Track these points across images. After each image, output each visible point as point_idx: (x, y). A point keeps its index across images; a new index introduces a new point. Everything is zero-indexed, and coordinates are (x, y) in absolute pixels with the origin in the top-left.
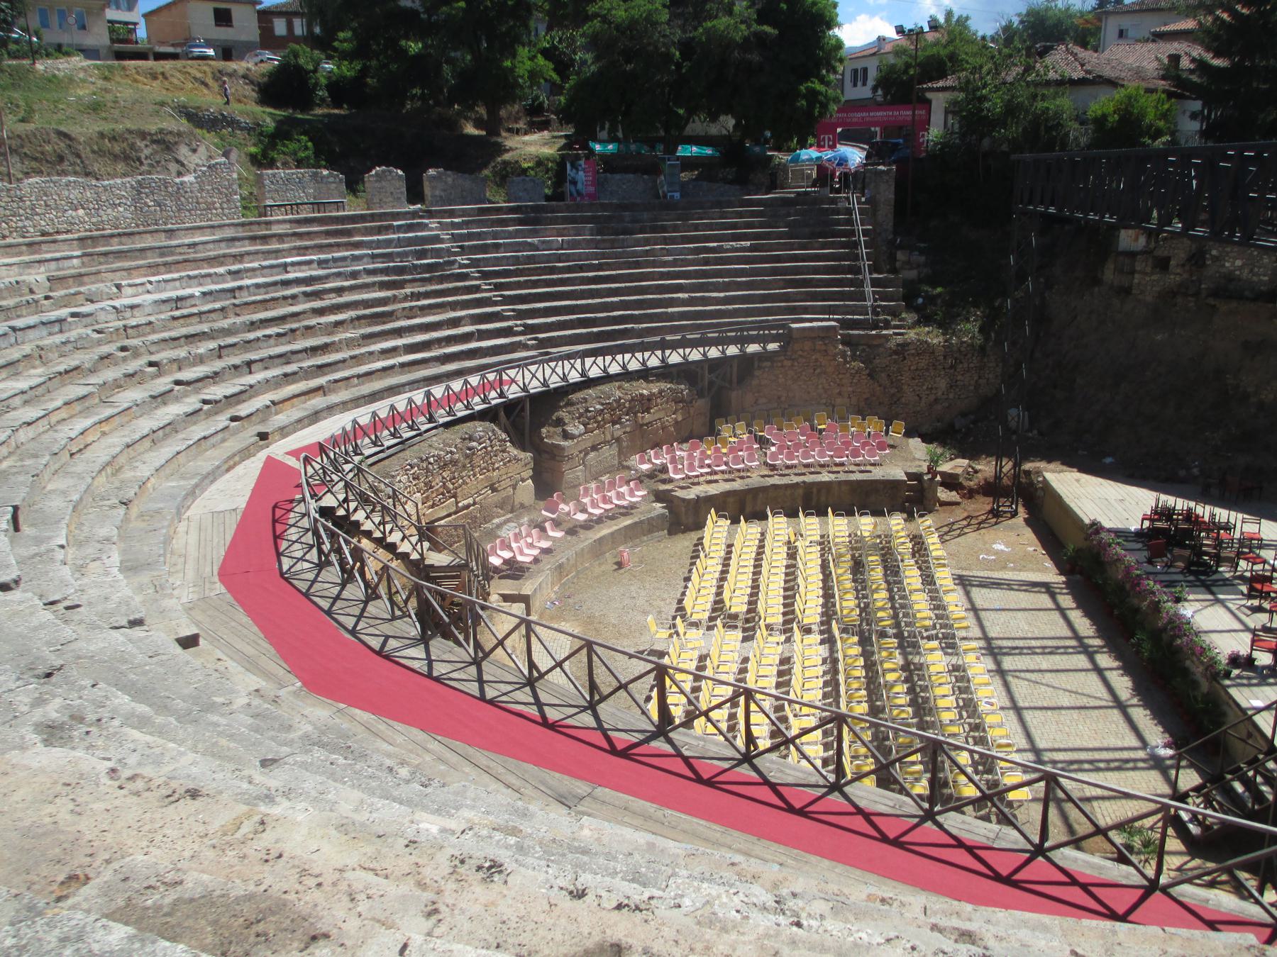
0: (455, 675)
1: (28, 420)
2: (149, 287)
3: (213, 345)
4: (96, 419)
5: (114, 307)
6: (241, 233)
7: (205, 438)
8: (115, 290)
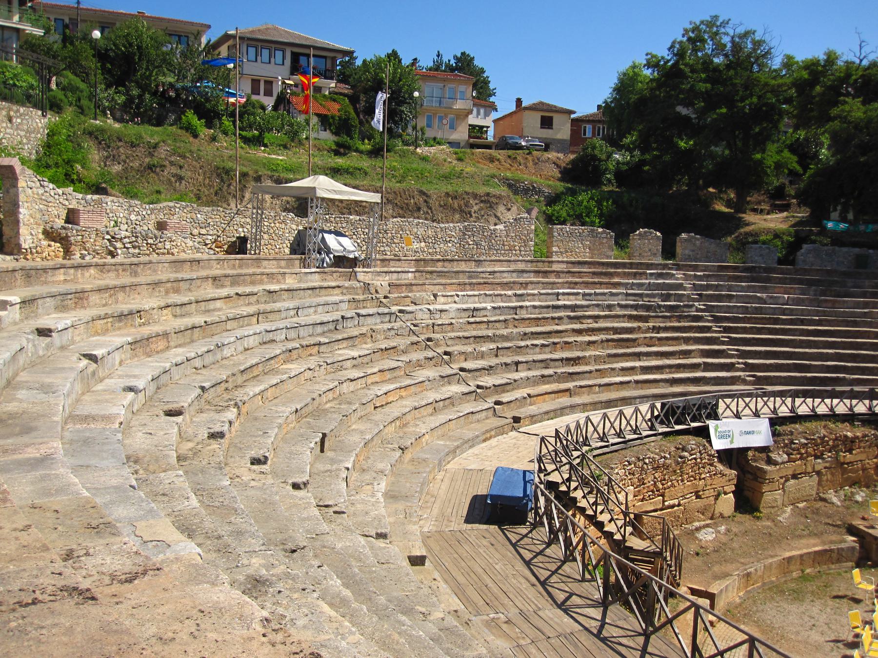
0: (624, 641)
1: (352, 378)
2: (456, 299)
3: (493, 346)
4: (398, 385)
5: (429, 310)
6: (529, 267)
7: (472, 413)
8: (432, 298)
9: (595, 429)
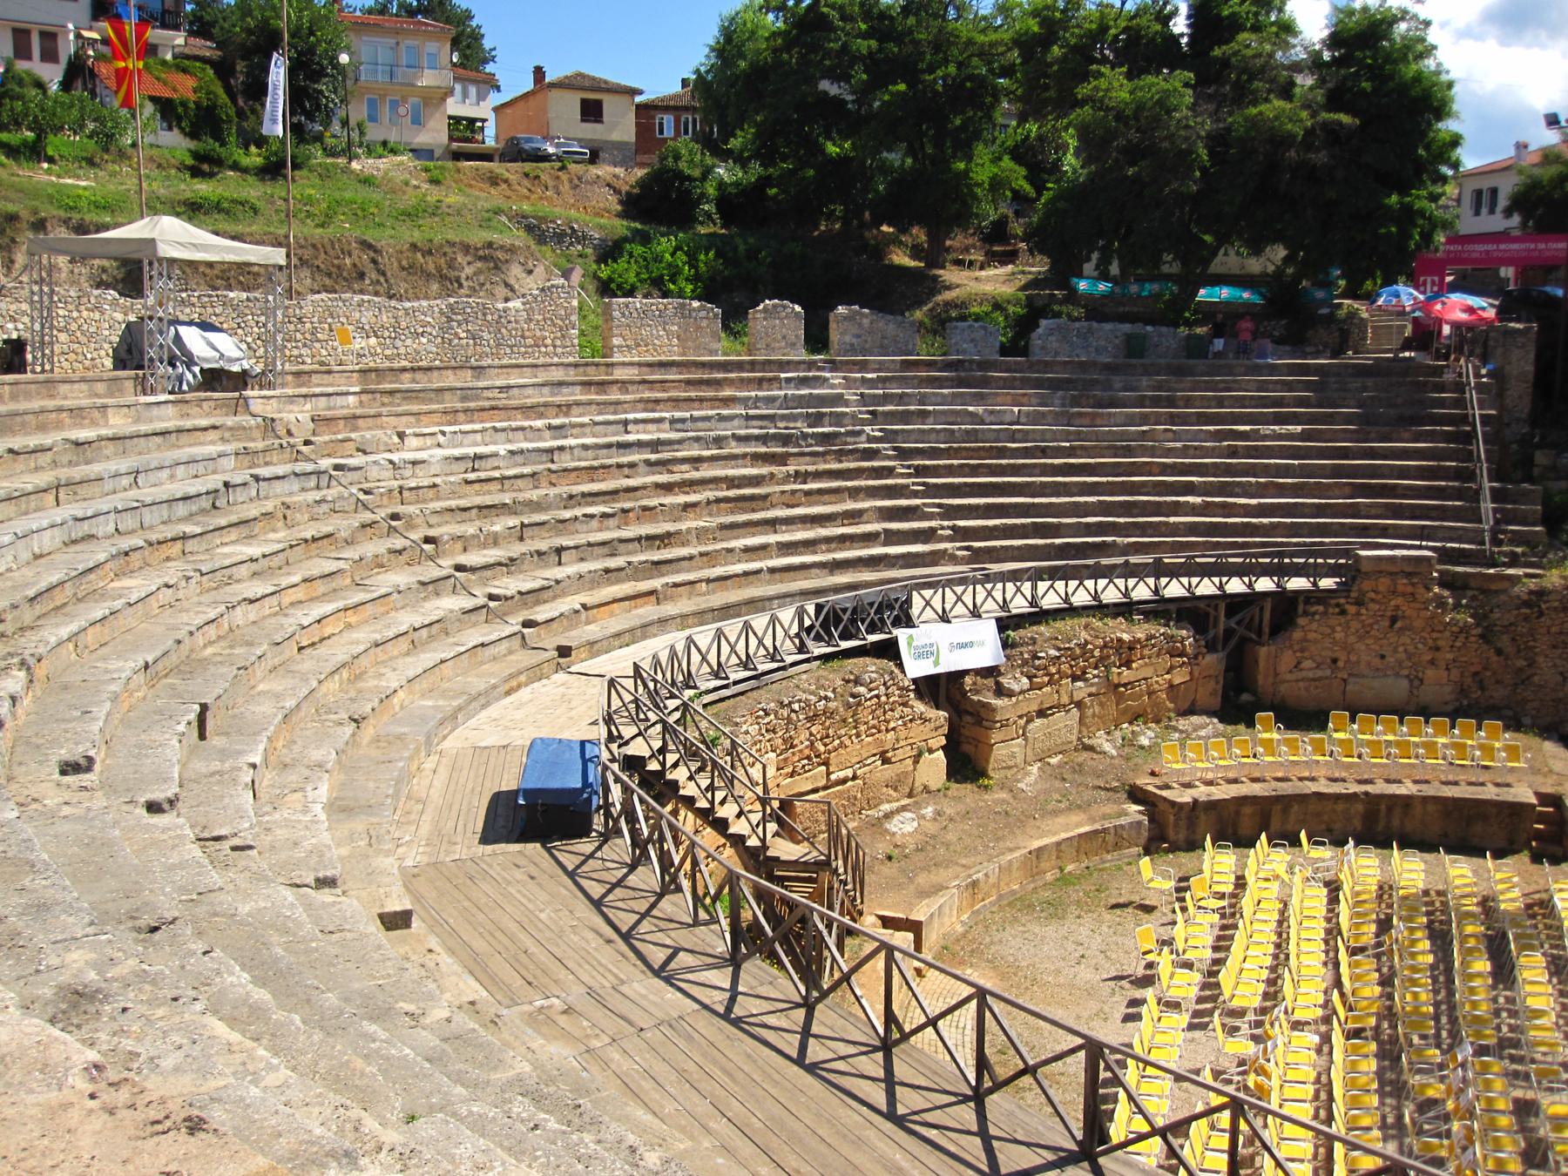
0: (771, 1020)
1: (251, 596)
2: (441, 439)
3: (513, 521)
4: (341, 604)
5: (391, 462)
6: (572, 375)
7: (483, 645)
8: (396, 439)
9: (704, 659)
